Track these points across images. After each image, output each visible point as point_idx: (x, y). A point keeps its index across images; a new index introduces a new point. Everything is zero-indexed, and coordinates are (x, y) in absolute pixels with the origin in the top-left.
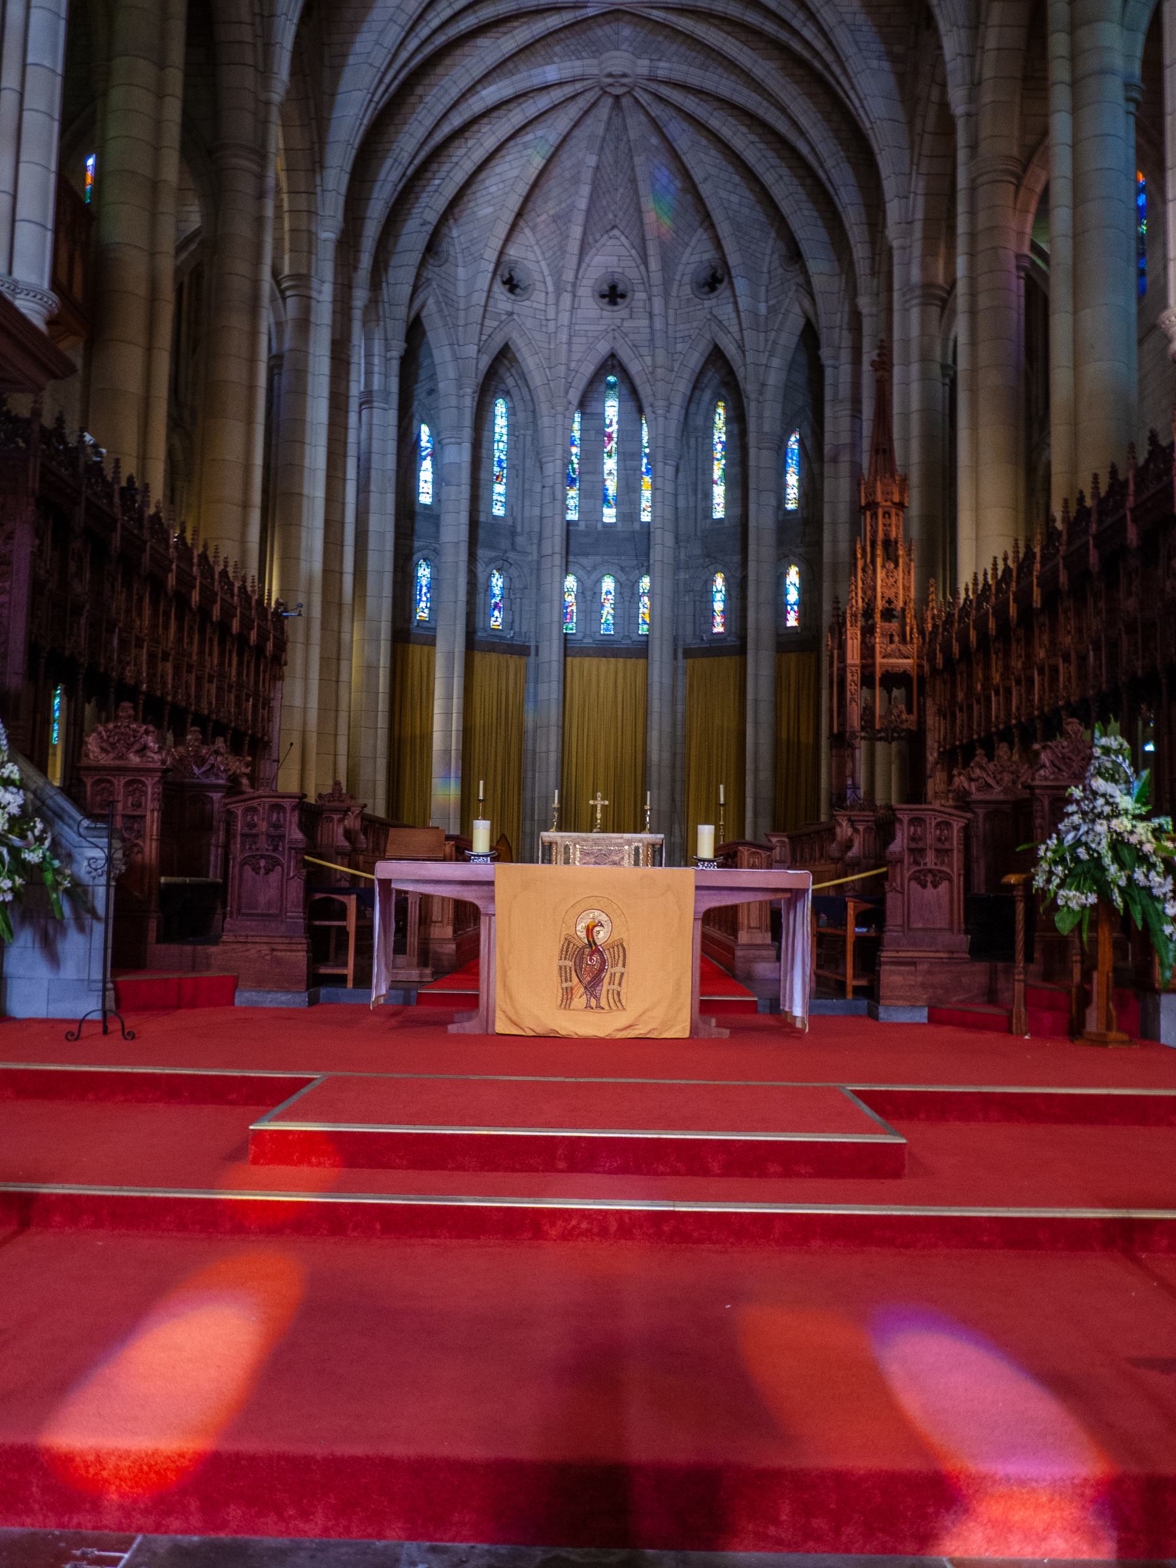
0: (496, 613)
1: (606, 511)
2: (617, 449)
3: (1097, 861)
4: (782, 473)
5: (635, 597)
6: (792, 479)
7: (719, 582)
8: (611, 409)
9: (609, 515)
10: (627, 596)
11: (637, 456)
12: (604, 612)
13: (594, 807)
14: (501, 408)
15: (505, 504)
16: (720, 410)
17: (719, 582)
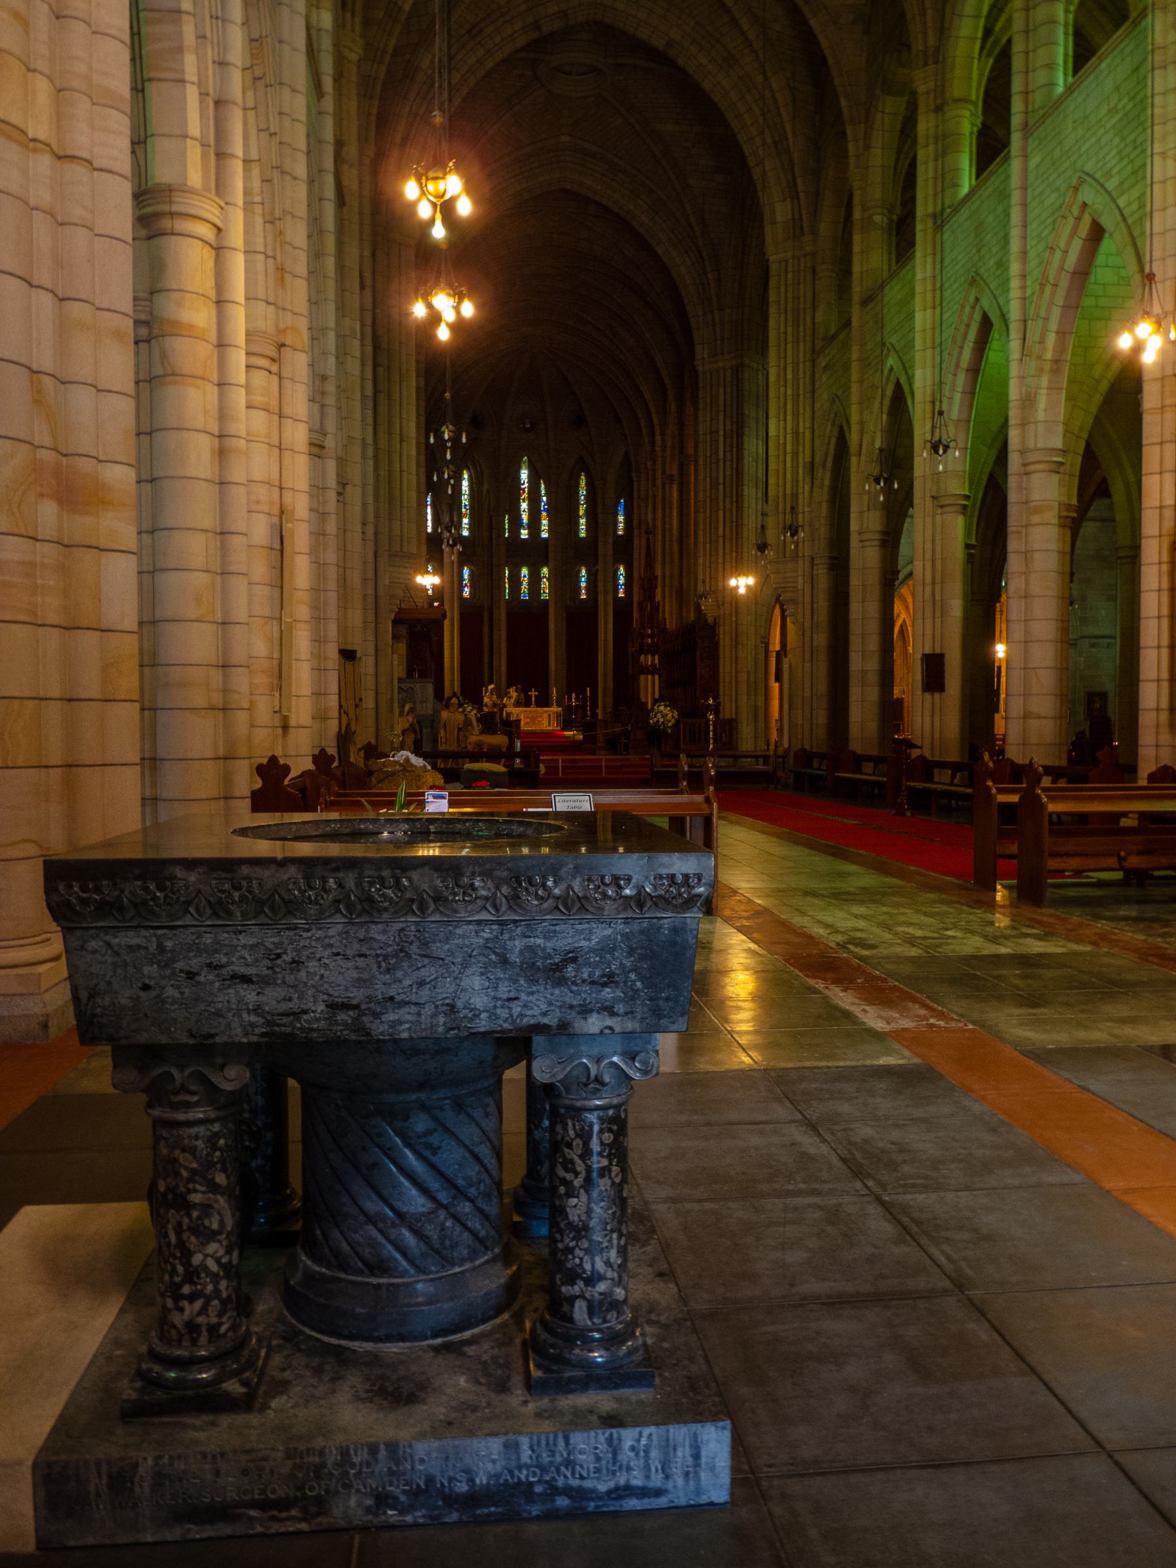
4: (616, 515)
6: (621, 518)
7: (584, 572)
8: (524, 475)
9: (524, 534)
10: (535, 579)
11: (540, 501)
15: (470, 530)
17: (584, 572)
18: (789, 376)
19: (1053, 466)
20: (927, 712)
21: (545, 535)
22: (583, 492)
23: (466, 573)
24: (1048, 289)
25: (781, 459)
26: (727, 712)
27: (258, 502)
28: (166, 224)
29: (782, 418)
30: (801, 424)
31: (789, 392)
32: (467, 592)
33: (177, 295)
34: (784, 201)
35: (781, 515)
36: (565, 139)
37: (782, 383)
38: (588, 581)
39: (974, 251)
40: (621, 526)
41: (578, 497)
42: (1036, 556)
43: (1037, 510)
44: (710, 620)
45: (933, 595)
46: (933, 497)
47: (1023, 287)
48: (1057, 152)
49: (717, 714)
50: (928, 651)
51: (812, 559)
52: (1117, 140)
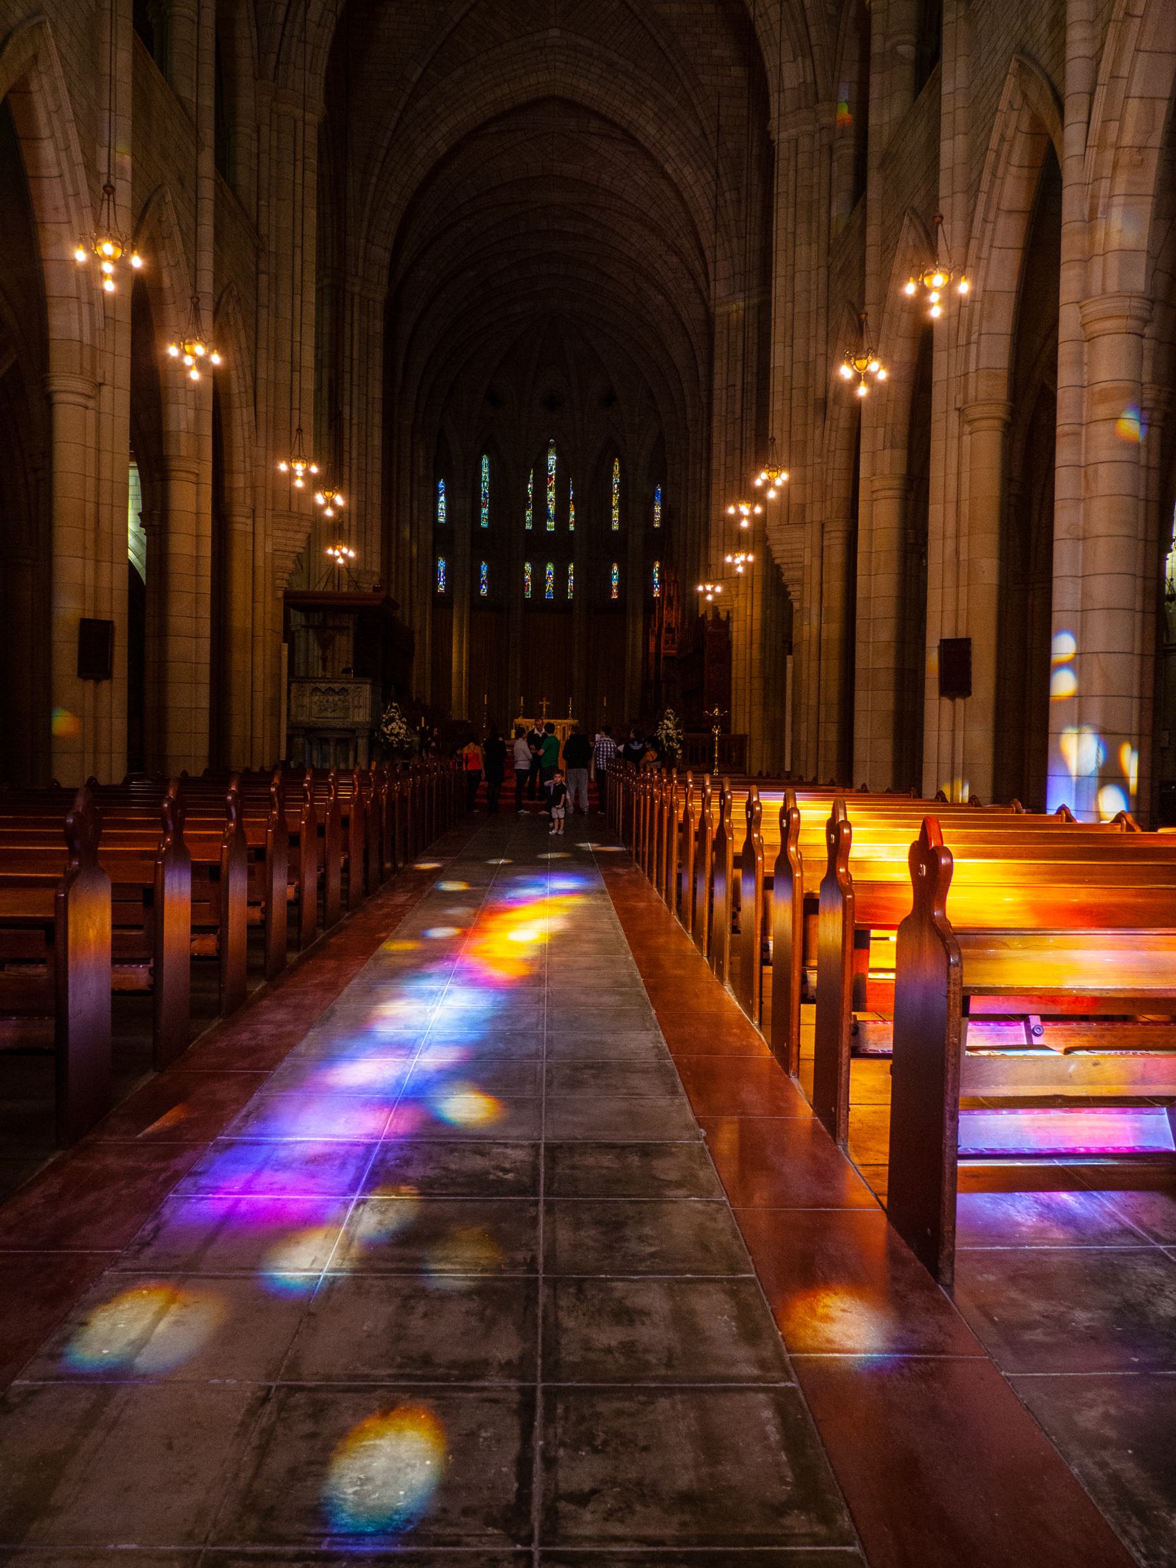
0: (484, 587)
1: (548, 523)
2: (556, 485)
3: (662, 740)
4: (652, 505)
5: (567, 576)
6: (658, 509)
7: (615, 569)
8: (552, 460)
9: (551, 526)
10: (561, 577)
12: (548, 585)
13: (541, 707)
14: (485, 461)
16: (617, 464)
17: (615, 569)
19: (1132, 323)
20: (946, 724)
21: (572, 527)
22: (616, 480)
23: (484, 568)
25: (787, 395)
26: (740, 726)
30: (812, 351)
32: (484, 591)
34: (795, 59)
36: (554, 32)
37: (789, 298)
38: (619, 580)
40: (657, 518)
41: (612, 485)
42: (1103, 470)
44: (723, 615)
45: (957, 552)
46: (959, 409)
49: (726, 729)
50: (948, 635)
51: (823, 525)
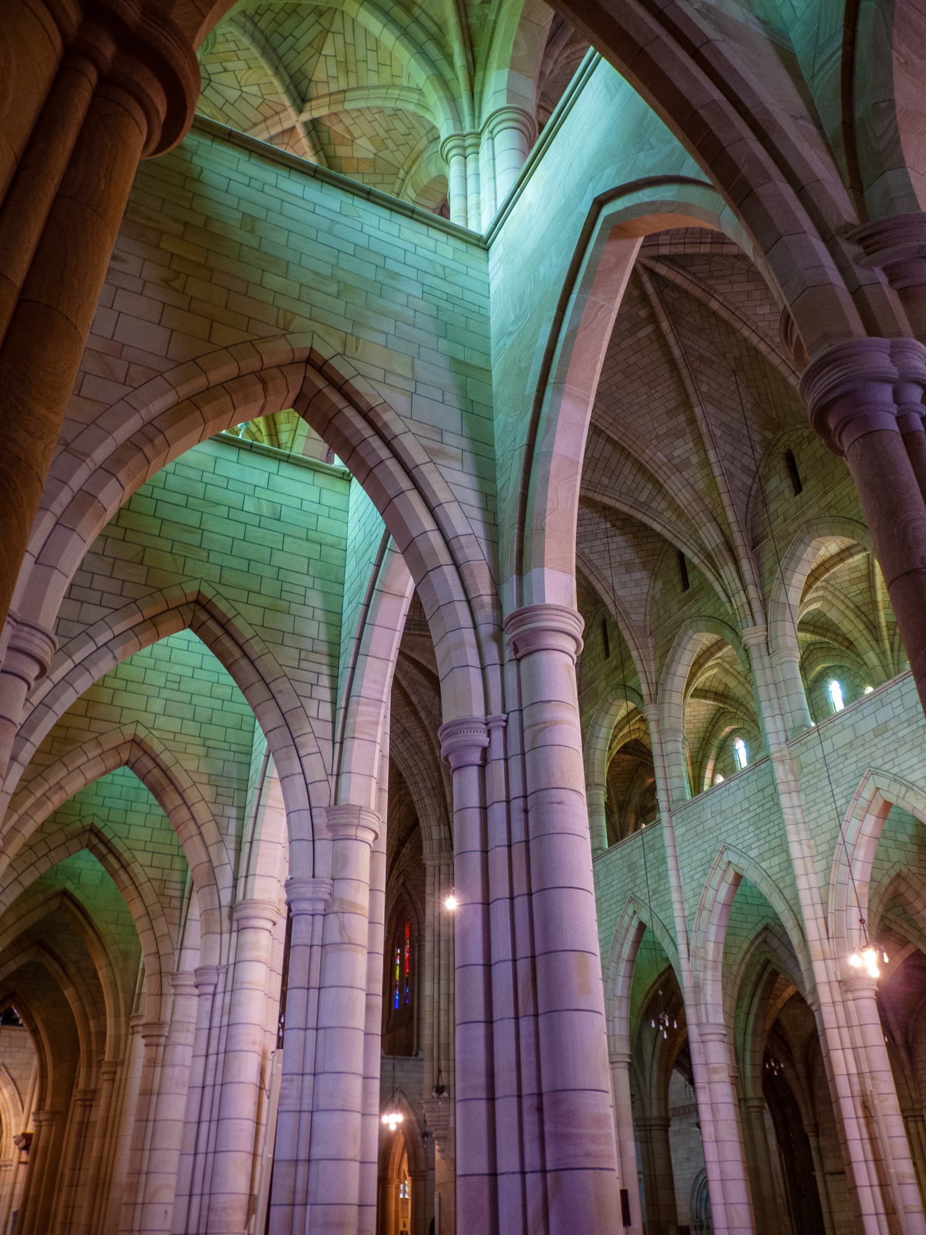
18: (442, 950)
19: (721, 1037)
24: (705, 913)
25: (436, 1014)
27: (254, 1043)
28: (352, 831)
29: (436, 981)
31: (442, 962)
33: (354, 883)
35: (435, 1062)
39: (629, 880)
42: (721, 1107)
43: (715, 1071)
47: (683, 909)
48: (700, 829)
52: (751, 828)
